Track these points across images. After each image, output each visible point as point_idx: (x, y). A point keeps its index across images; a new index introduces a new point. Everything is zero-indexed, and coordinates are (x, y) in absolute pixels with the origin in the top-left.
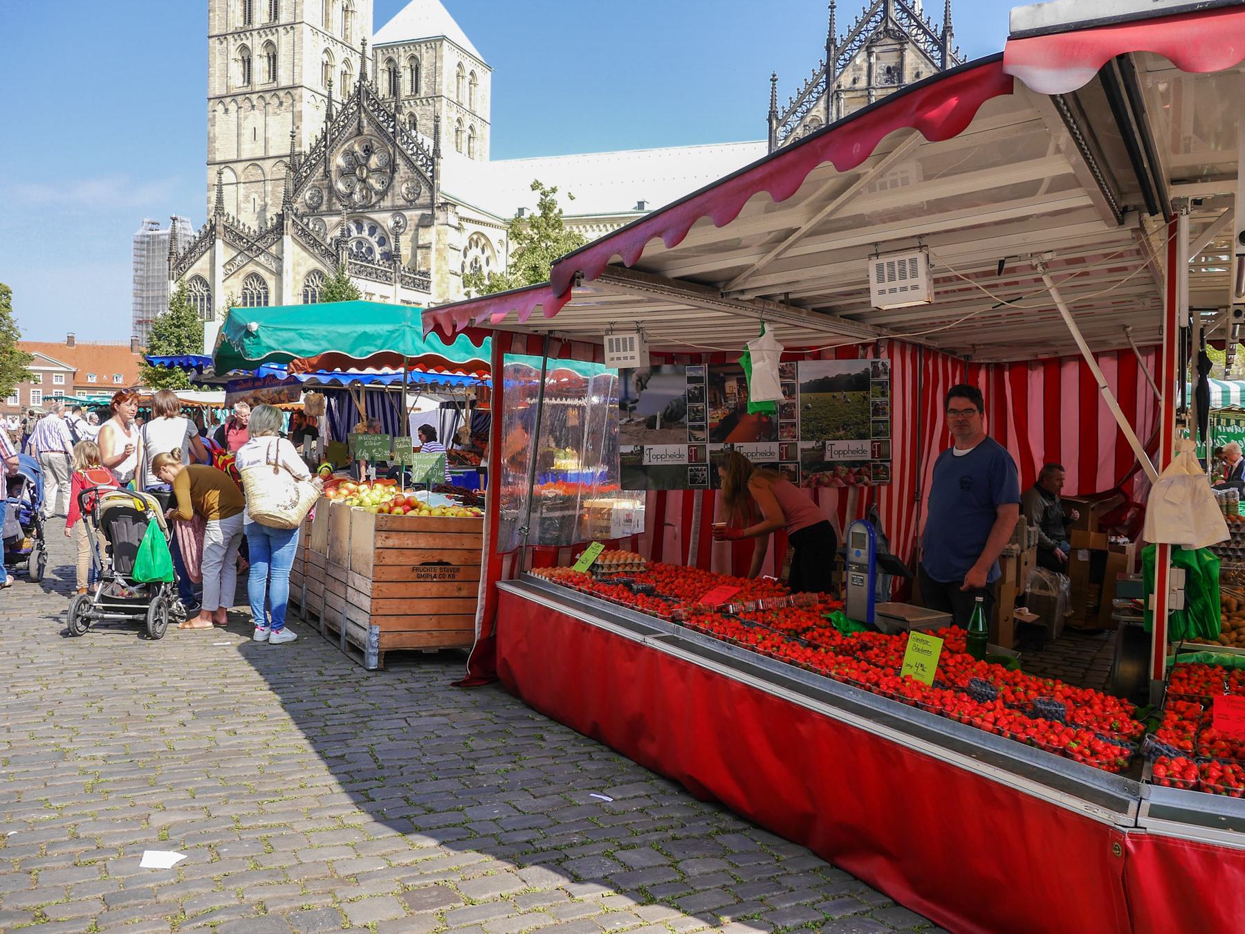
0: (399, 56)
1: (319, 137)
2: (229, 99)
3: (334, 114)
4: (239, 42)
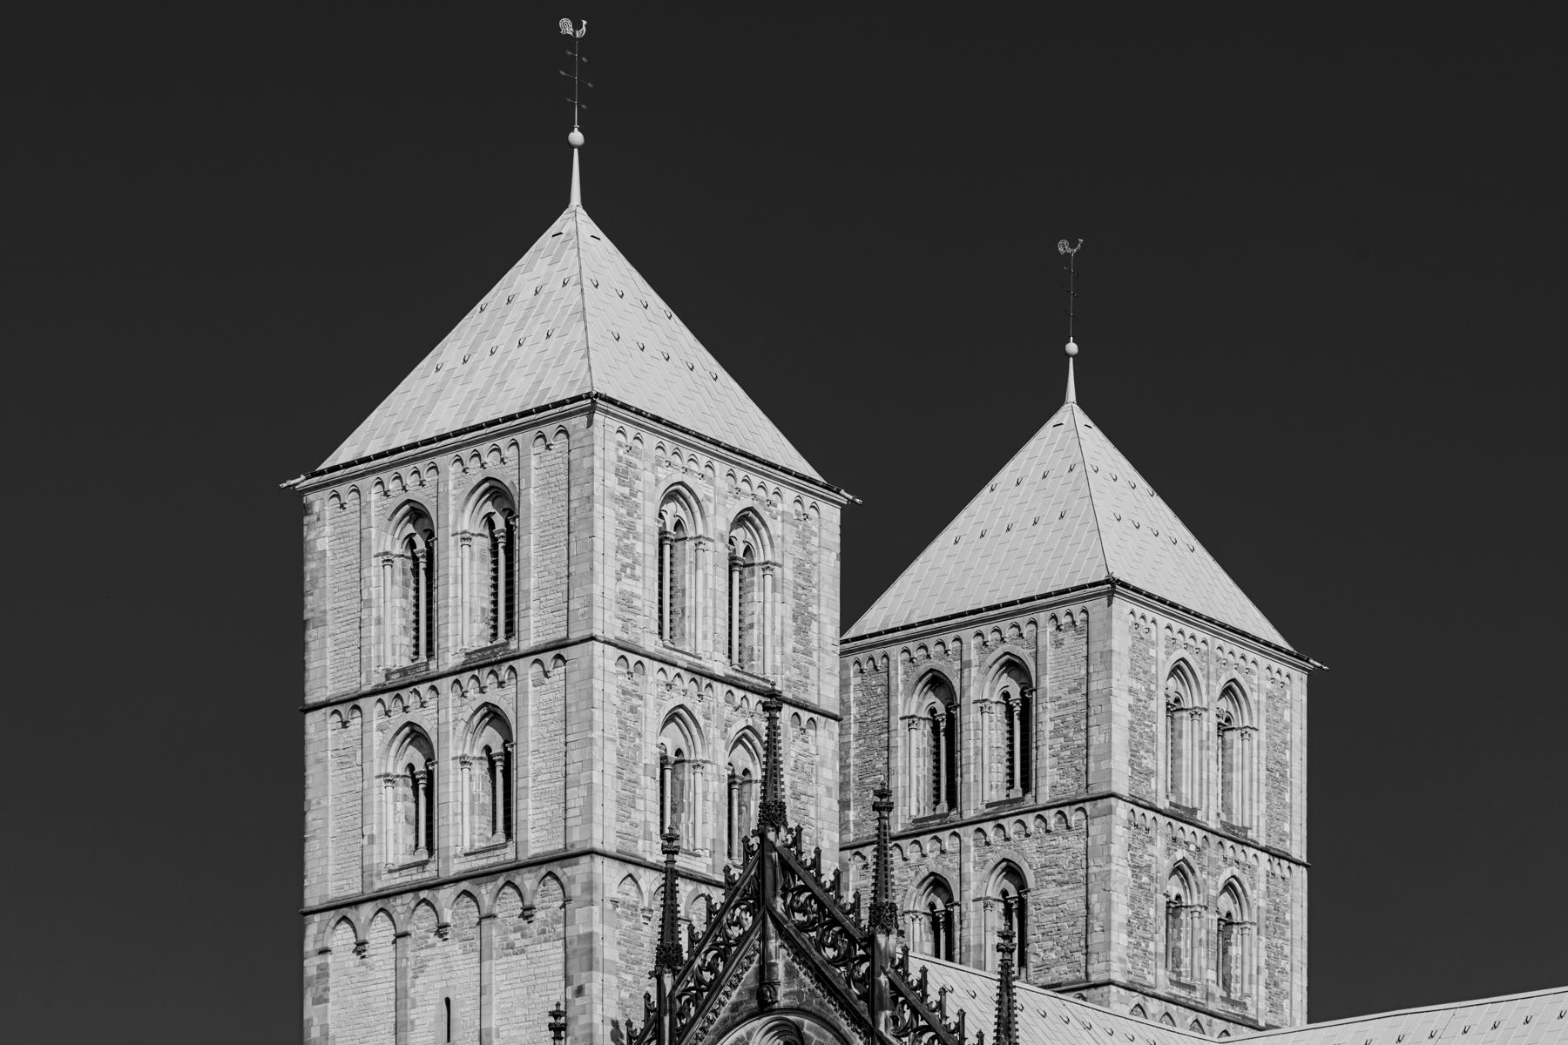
0: (965, 665)
1: (639, 1025)
2: (367, 910)
3: (684, 942)
4: (399, 719)
